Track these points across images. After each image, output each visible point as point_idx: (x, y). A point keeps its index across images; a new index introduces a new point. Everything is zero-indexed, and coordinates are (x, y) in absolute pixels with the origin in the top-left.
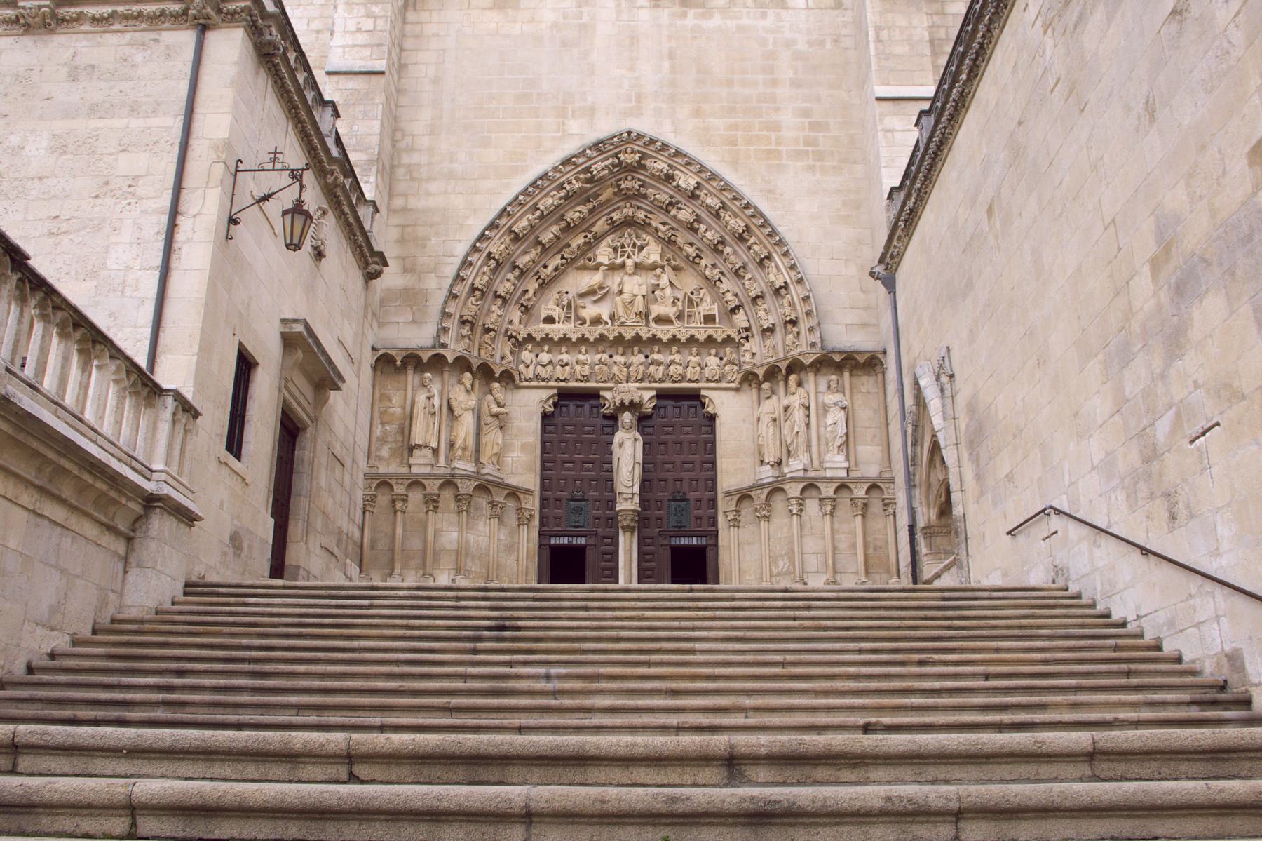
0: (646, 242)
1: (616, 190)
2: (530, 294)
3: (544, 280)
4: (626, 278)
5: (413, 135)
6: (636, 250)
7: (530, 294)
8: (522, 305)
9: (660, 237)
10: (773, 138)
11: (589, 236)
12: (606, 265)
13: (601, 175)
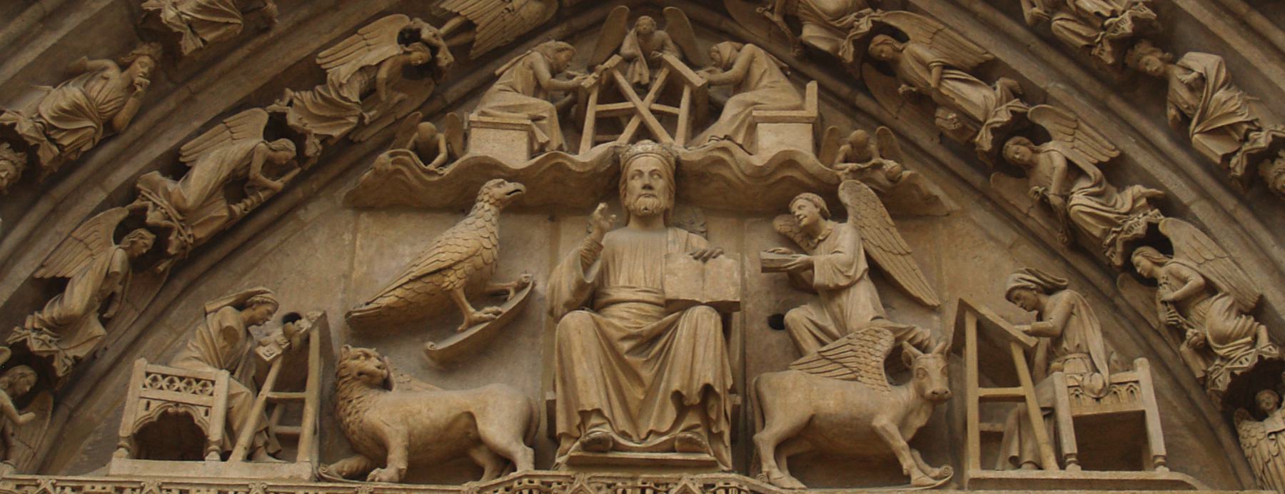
0: (737, 69)
2: (77, 298)
3: (162, 233)
4: (623, 239)
6: (683, 111)
7: (77, 298)
8: (21, 354)
9: (810, 54)
11: (427, 32)
12: (513, 176)
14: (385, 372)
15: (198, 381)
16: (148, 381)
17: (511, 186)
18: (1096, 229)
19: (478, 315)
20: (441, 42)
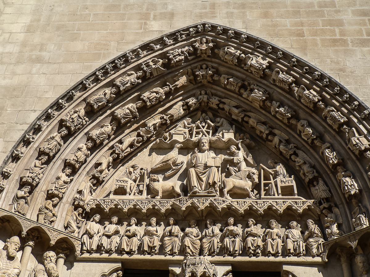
1: (192, 77)
2: (104, 166)
3: (118, 154)
5: (11, 33)
7: (104, 166)
8: (94, 177)
9: (234, 120)
10: (337, 30)
13: (177, 59)
14: (158, 179)
15: (125, 181)
16: (116, 181)
17: (180, 145)
18: (285, 152)
19: (174, 168)
20: (168, 119)
